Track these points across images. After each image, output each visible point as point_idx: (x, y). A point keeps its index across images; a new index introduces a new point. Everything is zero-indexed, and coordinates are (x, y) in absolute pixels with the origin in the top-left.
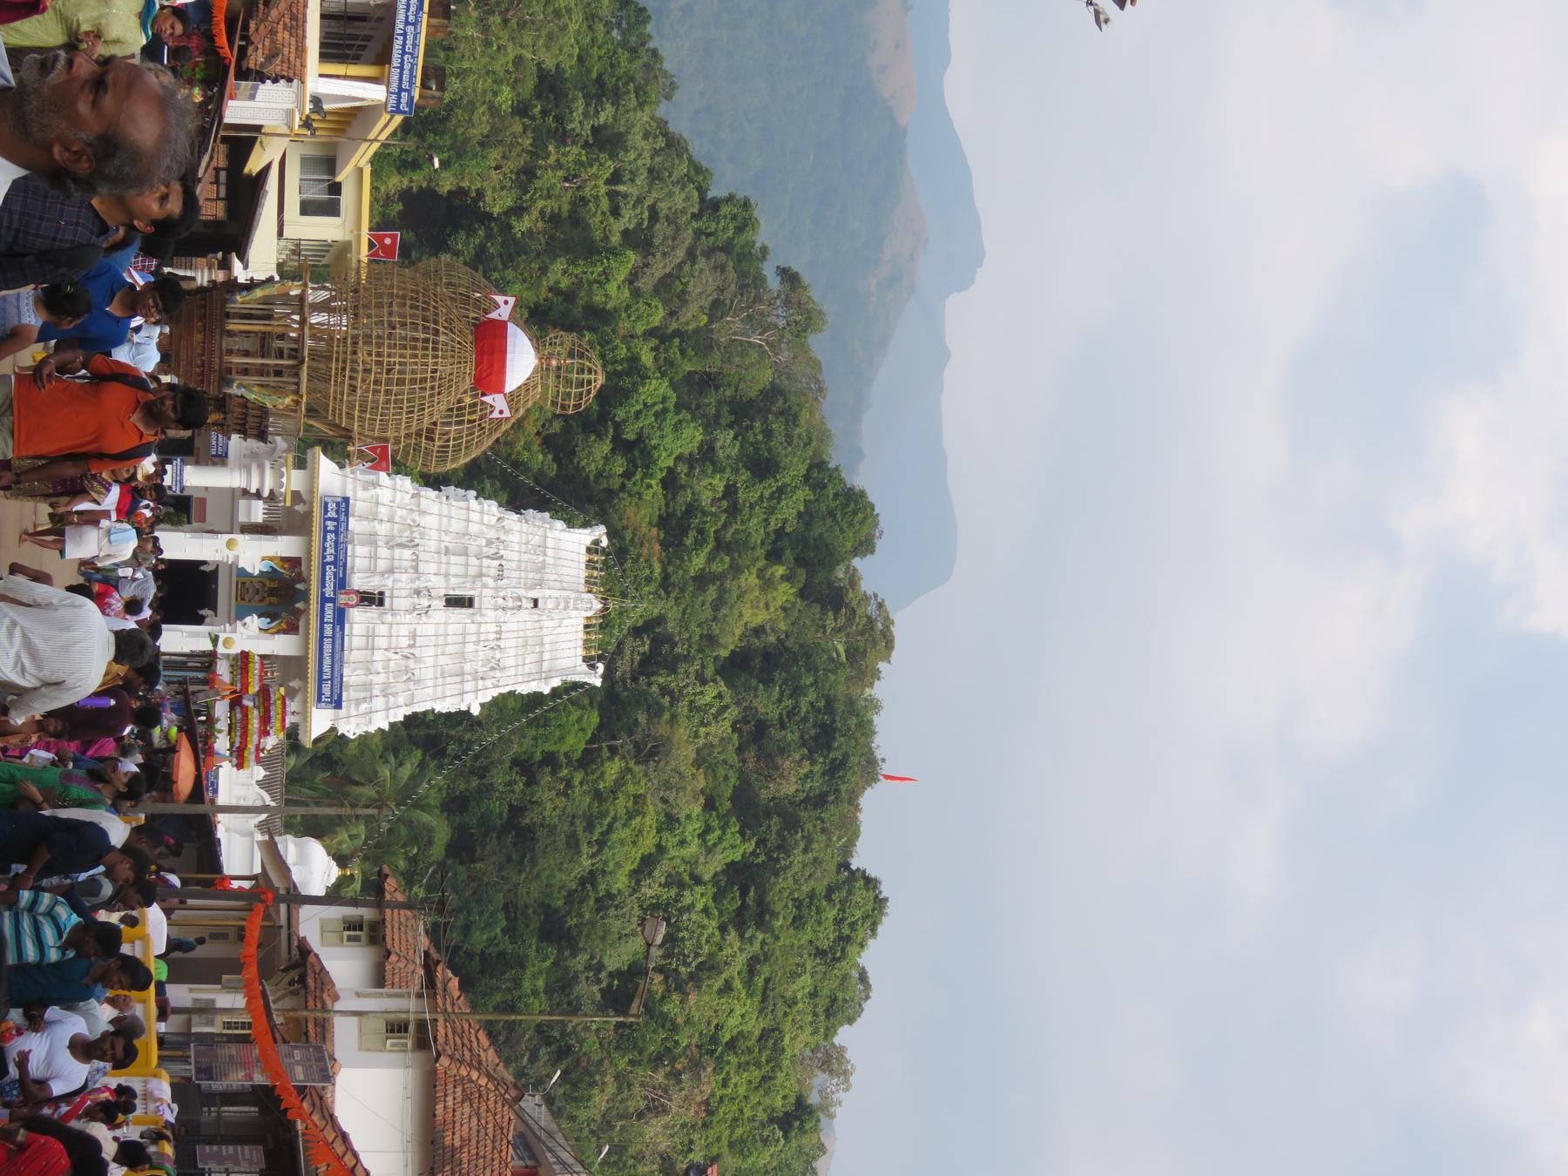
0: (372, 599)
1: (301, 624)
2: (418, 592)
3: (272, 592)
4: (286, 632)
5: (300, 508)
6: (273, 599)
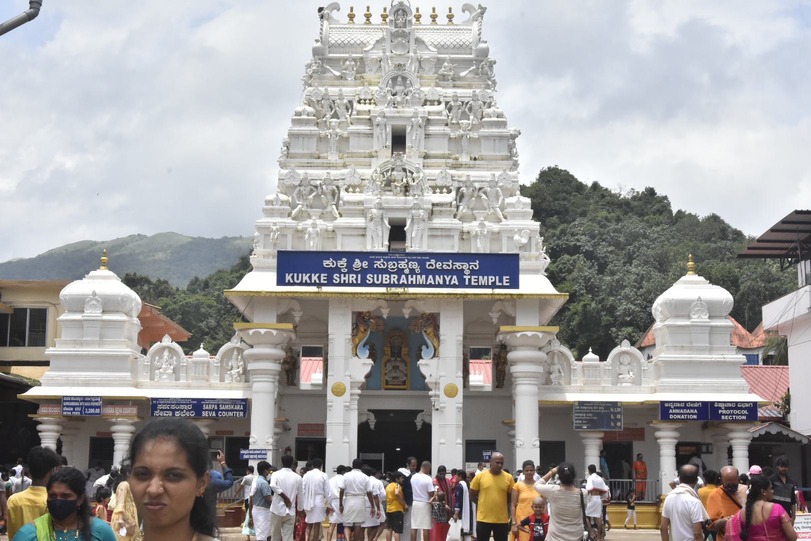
0: (397, 232)
1: (428, 310)
2: (389, 183)
3: (396, 353)
4: (437, 328)
5: (297, 316)
6: (404, 351)
